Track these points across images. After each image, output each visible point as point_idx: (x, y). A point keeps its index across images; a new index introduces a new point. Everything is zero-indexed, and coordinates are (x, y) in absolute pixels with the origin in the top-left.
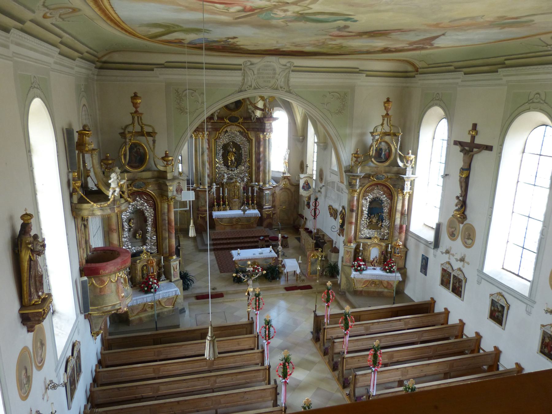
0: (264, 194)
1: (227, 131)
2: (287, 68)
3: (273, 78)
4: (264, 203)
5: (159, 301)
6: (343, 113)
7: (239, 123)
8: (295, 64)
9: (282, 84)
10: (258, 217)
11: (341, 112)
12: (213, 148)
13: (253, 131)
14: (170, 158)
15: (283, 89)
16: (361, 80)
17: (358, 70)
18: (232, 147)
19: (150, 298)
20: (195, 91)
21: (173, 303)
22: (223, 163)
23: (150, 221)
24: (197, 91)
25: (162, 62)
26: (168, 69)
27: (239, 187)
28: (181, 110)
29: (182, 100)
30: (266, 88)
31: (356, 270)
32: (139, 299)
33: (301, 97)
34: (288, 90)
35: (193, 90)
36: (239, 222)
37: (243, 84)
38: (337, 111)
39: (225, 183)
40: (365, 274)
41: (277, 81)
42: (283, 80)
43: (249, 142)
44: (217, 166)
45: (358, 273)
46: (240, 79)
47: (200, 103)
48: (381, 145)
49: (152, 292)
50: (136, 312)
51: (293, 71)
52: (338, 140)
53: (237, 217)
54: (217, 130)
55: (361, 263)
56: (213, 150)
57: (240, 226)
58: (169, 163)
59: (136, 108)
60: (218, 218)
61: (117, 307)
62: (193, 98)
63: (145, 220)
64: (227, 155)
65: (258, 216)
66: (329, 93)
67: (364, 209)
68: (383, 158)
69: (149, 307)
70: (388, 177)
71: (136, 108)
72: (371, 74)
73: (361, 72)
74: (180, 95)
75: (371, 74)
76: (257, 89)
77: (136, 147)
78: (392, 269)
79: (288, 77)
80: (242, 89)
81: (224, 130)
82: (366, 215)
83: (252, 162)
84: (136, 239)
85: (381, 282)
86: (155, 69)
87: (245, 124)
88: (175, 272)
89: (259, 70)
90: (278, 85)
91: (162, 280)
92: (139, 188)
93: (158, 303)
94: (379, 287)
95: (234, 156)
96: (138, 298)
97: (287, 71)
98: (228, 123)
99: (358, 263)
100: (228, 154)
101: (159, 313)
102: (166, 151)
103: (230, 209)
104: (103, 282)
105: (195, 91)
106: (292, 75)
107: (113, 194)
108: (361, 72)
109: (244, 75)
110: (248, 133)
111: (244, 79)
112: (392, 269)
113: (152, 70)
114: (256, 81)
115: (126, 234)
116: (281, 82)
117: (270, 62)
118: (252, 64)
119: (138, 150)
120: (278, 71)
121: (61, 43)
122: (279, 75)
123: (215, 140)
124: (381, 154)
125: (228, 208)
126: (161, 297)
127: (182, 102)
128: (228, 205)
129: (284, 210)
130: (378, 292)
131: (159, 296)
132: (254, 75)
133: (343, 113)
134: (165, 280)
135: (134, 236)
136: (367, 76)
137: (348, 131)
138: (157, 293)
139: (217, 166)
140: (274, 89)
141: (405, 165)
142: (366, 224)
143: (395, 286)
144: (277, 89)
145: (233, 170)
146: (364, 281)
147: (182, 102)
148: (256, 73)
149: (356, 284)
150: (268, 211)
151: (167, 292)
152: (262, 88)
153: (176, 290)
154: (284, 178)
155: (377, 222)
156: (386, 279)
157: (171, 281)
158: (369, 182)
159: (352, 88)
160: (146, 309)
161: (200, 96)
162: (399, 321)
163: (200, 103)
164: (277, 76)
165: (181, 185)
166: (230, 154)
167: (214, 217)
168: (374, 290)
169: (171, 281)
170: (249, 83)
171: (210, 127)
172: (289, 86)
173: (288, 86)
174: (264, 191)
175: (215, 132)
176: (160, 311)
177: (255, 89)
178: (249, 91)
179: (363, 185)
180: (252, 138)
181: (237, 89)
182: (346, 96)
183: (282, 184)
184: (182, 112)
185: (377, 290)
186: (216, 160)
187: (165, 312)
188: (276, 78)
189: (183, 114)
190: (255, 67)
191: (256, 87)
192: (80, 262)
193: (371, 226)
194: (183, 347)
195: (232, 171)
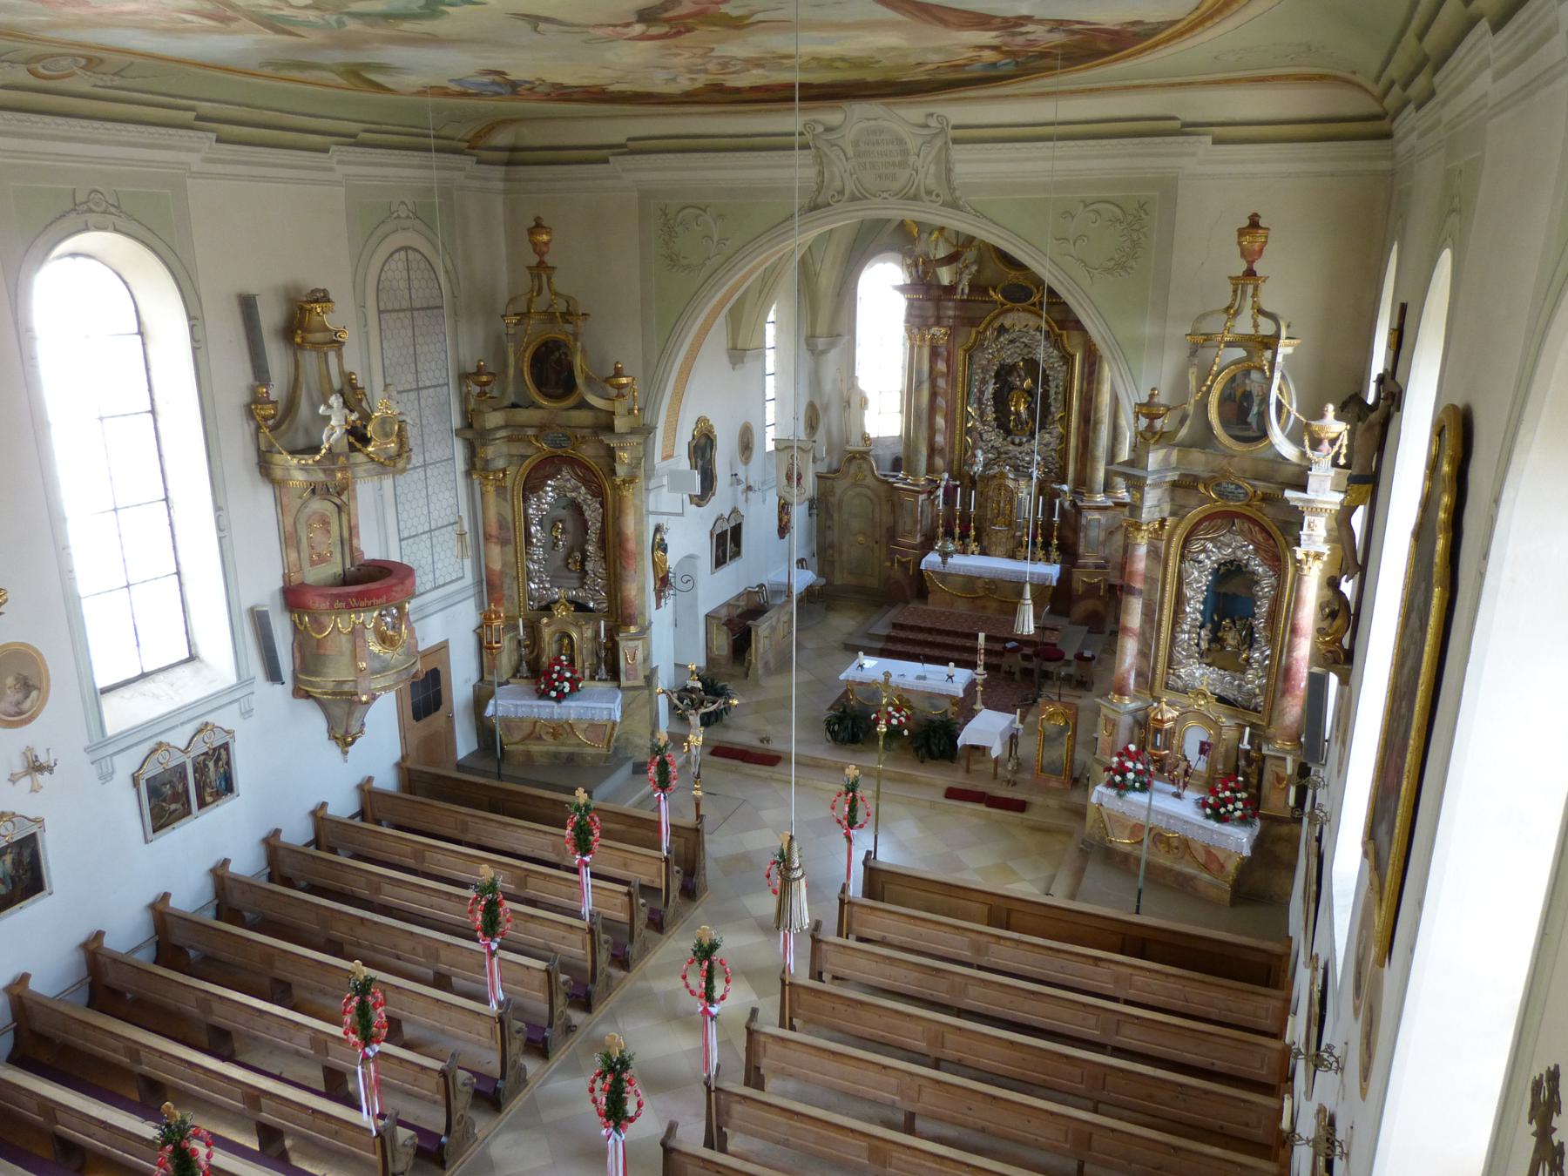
0: (1084, 522)
1: (1002, 330)
2: (936, 135)
3: (904, 164)
5: (570, 725)
6: (1131, 268)
7: (1034, 304)
8: (953, 121)
9: (931, 183)
10: (1048, 587)
11: (1124, 268)
14: (624, 381)
15: (934, 198)
16: (1199, 156)
17: (1177, 124)
18: (1023, 373)
20: (705, 211)
22: (995, 419)
23: (593, 536)
24: (708, 210)
25: (621, 139)
26: (637, 157)
29: (673, 234)
30: (885, 195)
31: (1111, 784)
32: (522, 706)
33: (991, 220)
34: (949, 198)
35: (701, 209)
36: (995, 593)
37: (822, 188)
38: (1113, 263)
40: (1131, 803)
41: (914, 173)
42: (932, 169)
43: (1066, 363)
44: (969, 425)
45: (1112, 792)
46: (812, 172)
48: (1247, 381)
50: (517, 737)
51: (956, 141)
52: (1114, 358)
53: (986, 575)
54: (972, 322)
55: (1130, 764)
57: (995, 605)
58: (624, 391)
59: (541, 254)
60: (933, 572)
61: (346, 688)
62: (699, 228)
65: (1048, 583)
66: (1082, 205)
67: (1189, 593)
68: (1254, 425)
69: (547, 733)
70: (1255, 492)
71: (541, 254)
72: (1229, 134)
73: (1189, 129)
74: (671, 222)
75: (1229, 134)
76: (859, 199)
77: (559, 349)
78: (1222, 810)
79: (947, 161)
80: (819, 200)
81: (996, 325)
82: (1198, 616)
83: (1069, 421)
84: (570, 570)
85: (1185, 846)
86: (611, 159)
88: (629, 666)
89: (856, 144)
90: (918, 185)
91: (600, 680)
94: (1182, 858)
96: (518, 702)
97: (939, 143)
98: (1003, 305)
99: (1121, 764)
101: (573, 754)
102: (617, 363)
103: (984, 552)
104: (321, 629)
105: (705, 211)
106: (959, 153)
107: (329, 439)
108: (1189, 129)
109: (821, 161)
110: (1061, 335)
111: (821, 173)
112: (1222, 810)
113: (606, 161)
114: (854, 176)
115: (538, 553)
116: (928, 177)
117: (875, 119)
118: (829, 129)
119: (563, 357)
120: (912, 144)
121: (198, 118)
122: (919, 156)
123: (966, 351)
124: (1247, 412)
125: (973, 546)
126: (573, 716)
127: (675, 240)
128: (978, 539)
130: (1179, 874)
131: (569, 714)
132: (847, 159)
133: (1131, 268)
134: (606, 680)
136: (1217, 141)
137: (1148, 329)
138: (565, 703)
139: (969, 425)
140: (908, 199)
141: (1303, 454)
142: (1198, 645)
143: (1231, 867)
144: (915, 198)
145: (1017, 441)
146: (1131, 824)
148: (850, 153)
149: (1108, 827)
150: (1090, 575)
152: (875, 196)
155: (1237, 647)
156: (1201, 838)
158: (1202, 502)
159: (1168, 188)
162: (1091, 961)
164: (912, 159)
166: (1014, 395)
167: (923, 567)
168: (1168, 864)
170: (838, 184)
171: (951, 313)
172: (952, 190)
173: (950, 189)
174: (1085, 513)
176: (576, 750)
177: (853, 198)
178: (836, 205)
179: (1182, 512)
182: (1142, 213)
185: (1177, 867)
186: (969, 409)
188: (911, 163)
190: (843, 136)
191: (857, 194)
192: (284, 575)
193: (1214, 653)
194: (510, 829)
195: (1013, 443)
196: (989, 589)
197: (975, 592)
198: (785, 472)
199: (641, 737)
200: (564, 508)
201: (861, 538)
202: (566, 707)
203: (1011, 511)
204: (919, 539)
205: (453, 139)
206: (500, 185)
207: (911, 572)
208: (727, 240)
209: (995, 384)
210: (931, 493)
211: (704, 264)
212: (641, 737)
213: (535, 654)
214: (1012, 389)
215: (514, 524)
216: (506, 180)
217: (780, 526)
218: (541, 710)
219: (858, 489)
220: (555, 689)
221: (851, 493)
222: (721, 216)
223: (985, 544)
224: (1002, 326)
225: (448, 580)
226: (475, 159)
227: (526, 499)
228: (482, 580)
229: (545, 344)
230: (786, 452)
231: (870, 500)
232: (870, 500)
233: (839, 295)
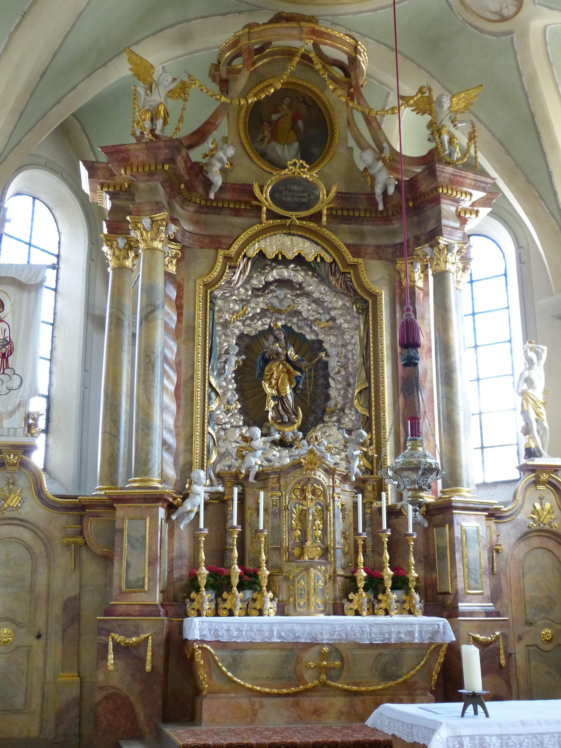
4: (460, 585)
10: (440, 646)
12: (199, 322)
13: (380, 259)
27: (324, 493)
36: (337, 678)
39: (251, 479)
43: (364, 311)
44: (214, 407)
53: (325, 638)
56: (199, 330)
60: (219, 645)
64: (262, 375)
65: (439, 640)
81: (252, 251)
87: (344, 227)
95: (291, 383)
98: (271, 215)
100: (263, 369)
110: (355, 266)
123: (207, 286)
129: (548, 647)
154: (531, 477)
175: (212, 252)
180: (375, 289)
183: (528, 508)
196: (327, 670)
197: (300, 679)
203: (324, 531)
204: (158, 598)
207: (148, 668)
209: (238, 355)
210: (171, 508)
214: (266, 361)
223: (283, 596)
224: (261, 254)
231: (28, 548)
232: (28, 548)
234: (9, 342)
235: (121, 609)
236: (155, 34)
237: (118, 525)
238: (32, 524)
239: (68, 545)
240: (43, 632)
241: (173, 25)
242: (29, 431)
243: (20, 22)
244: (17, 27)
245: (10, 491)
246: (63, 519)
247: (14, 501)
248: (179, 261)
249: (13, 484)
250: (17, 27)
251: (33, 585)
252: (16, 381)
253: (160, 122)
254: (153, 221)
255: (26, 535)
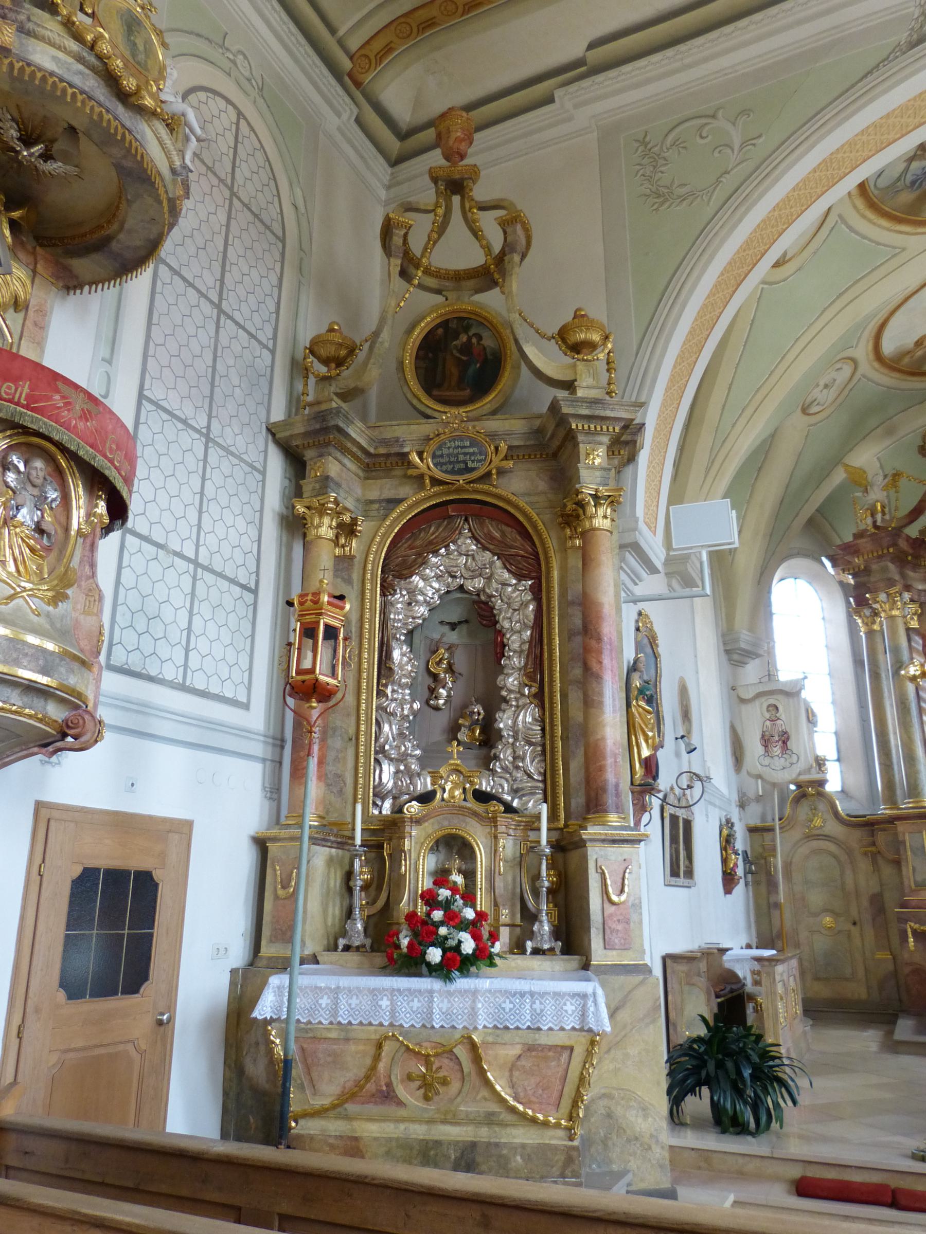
5: (473, 1047)
19: (416, 1004)
20: (714, 116)
21: (569, 1090)
24: (720, 114)
25: (575, 49)
26: (600, 78)
28: (659, 196)
32: (350, 991)
47: (736, 148)
49: (433, 970)
63: (499, 649)
69: (410, 1078)
77: (466, 329)
86: (558, 94)
88: (610, 909)
91: (536, 952)
92: (460, 472)
93: (462, 1052)
96: (346, 981)
101: (473, 1145)
113: (550, 100)
119: (474, 340)
127: (663, 169)
131: (473, 1013)
135: (453, 731)
147: (663, 169)
151: (522, 995)
153: (584, 996)
157: (586, 966)
160: (389, 1085)
161: (734, 124)
163: (736, 148)
165: (782, 713)
169: (586, 966)
176: (483, 1134)
181: (903, 37)
184: (666, 200)
187: (514, 1148)
189: (668, 204)
198: (759, 736)
199: (645, 1110)
200: (453, 626)
201: (828, 920)
202: (463, 993)
205: (333, 31)
206: (383, 194)
208: (760, 136)
211: (718, 181)
212: (645, 1110)
213: (381, 903)
215: (361, 628)
216: (388, 188)
217: (725, 873)
218: (401, 1001)
219: (815, 844)
220: (441, 943)
221: (804, 850)
222: (745, 112)
225: (214, 690)
226: (356, 111)
227: (387, 589)
228: (283, 740)
229: (445, 324)
230: (757, 703)
231: (835, 857)
232: (835, 857)
233: (759, 583)
234: (786, 733)
235: (914, 904)
236: (864, 438)
237: (901, 838)
238: (835, 838)
239: (865, 854)
240: (857, 919)
241: (878, 427)
242: (820, 769)
243: (758, 475)
244: (756, 479)
245: (814, 815)
246: (857, 834)
247: (818, 822)
248: (920, 616)
249: (815, 809)
250: (756, 479)
251: (843, 884)
252: (795, 758)
253: (879, 517)
254: (888, 595)
255: (832, 847)
